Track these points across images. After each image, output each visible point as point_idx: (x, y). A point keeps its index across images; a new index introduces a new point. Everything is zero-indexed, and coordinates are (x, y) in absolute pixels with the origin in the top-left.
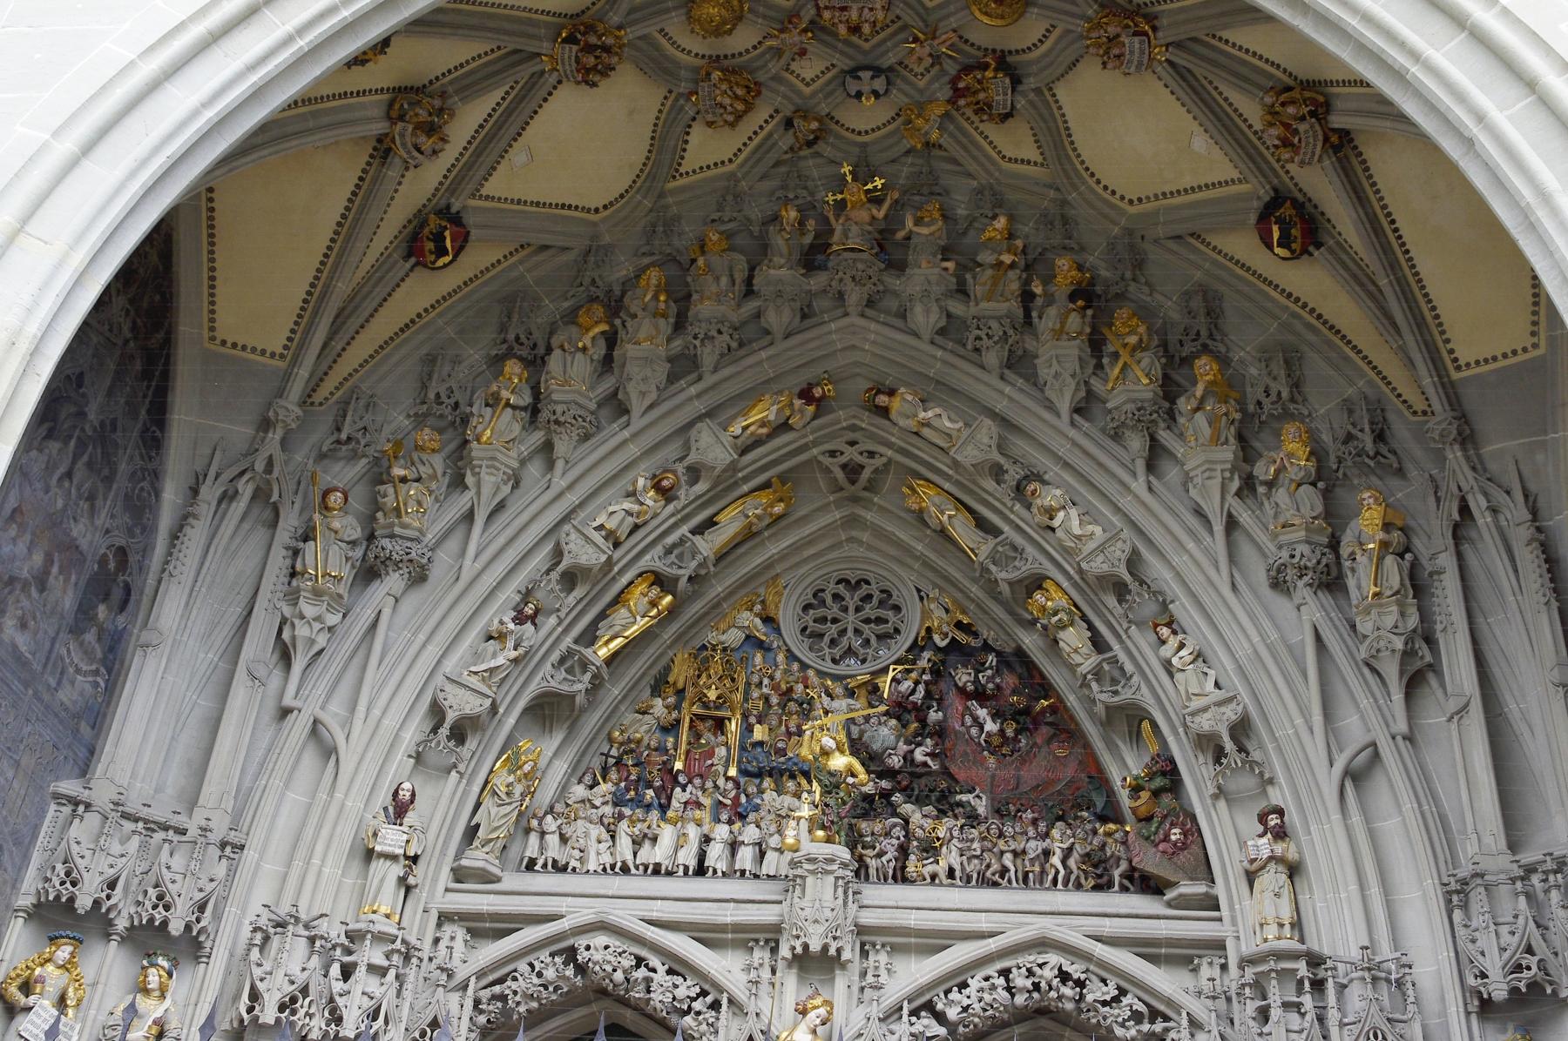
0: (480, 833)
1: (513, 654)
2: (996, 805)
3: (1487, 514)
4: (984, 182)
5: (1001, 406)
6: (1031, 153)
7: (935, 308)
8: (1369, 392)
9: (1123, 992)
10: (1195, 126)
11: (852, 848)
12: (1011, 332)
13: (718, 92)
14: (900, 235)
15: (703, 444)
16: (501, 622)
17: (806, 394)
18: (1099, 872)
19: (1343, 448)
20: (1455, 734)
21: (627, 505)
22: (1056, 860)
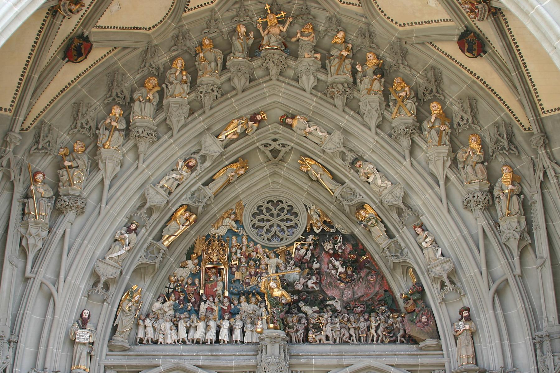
1: (128, 248)
3: (554, 178)
4: (332, 14)
7: (312, 78)
8: (505, 118)
11: (284, 330)
12: (348, 90)
14: (294, 40)
15: (207, 144)
16: (121, 234)
17: (253, 119)
18: (391, 335)
21: (174, 176)
22: (373, 331)
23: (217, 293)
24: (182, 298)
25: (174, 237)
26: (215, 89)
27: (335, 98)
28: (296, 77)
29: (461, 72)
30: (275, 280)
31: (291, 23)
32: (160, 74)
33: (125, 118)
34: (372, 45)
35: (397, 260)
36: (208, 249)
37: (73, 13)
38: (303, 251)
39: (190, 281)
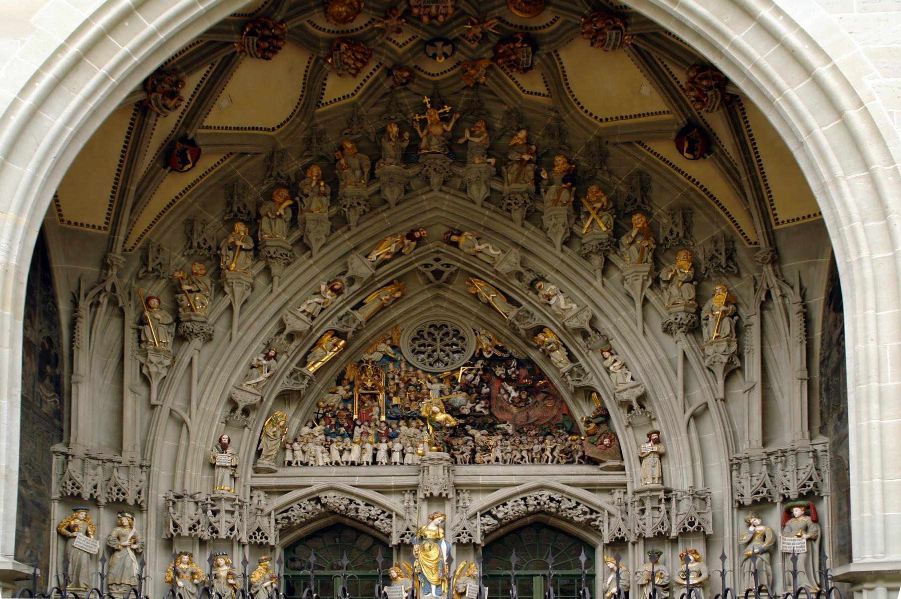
0: (263, 452)
1: (268, 375)
2: (518, 429)
4: (512, 107)
5: (522, 241)
6: (542, 89)
8: (728, 234)
9: (578, 504)
10: (645, 81)
12: (528, 201)
13: (345, 56)
14: (461, 141)
15: (354, 265)
16: (258, 360)
19: (709, 263)
20: (746, 399)
21: (317, 300)
22: (548, 453)
23: (373, 417)
24: (333, 423)
25: (320, 363)
26: (361, 202)
27: (513, 211)
28: (464, 187)
29: (677, 178)
30: (437, 405)
31: (457, 121)
32: (291, 185)
33: (251, 236)
34: (562, 146)
35: (580, 384)
36: (361, 375)
37: (168, 109)
38: (470, 376)
39: (341, 407)
